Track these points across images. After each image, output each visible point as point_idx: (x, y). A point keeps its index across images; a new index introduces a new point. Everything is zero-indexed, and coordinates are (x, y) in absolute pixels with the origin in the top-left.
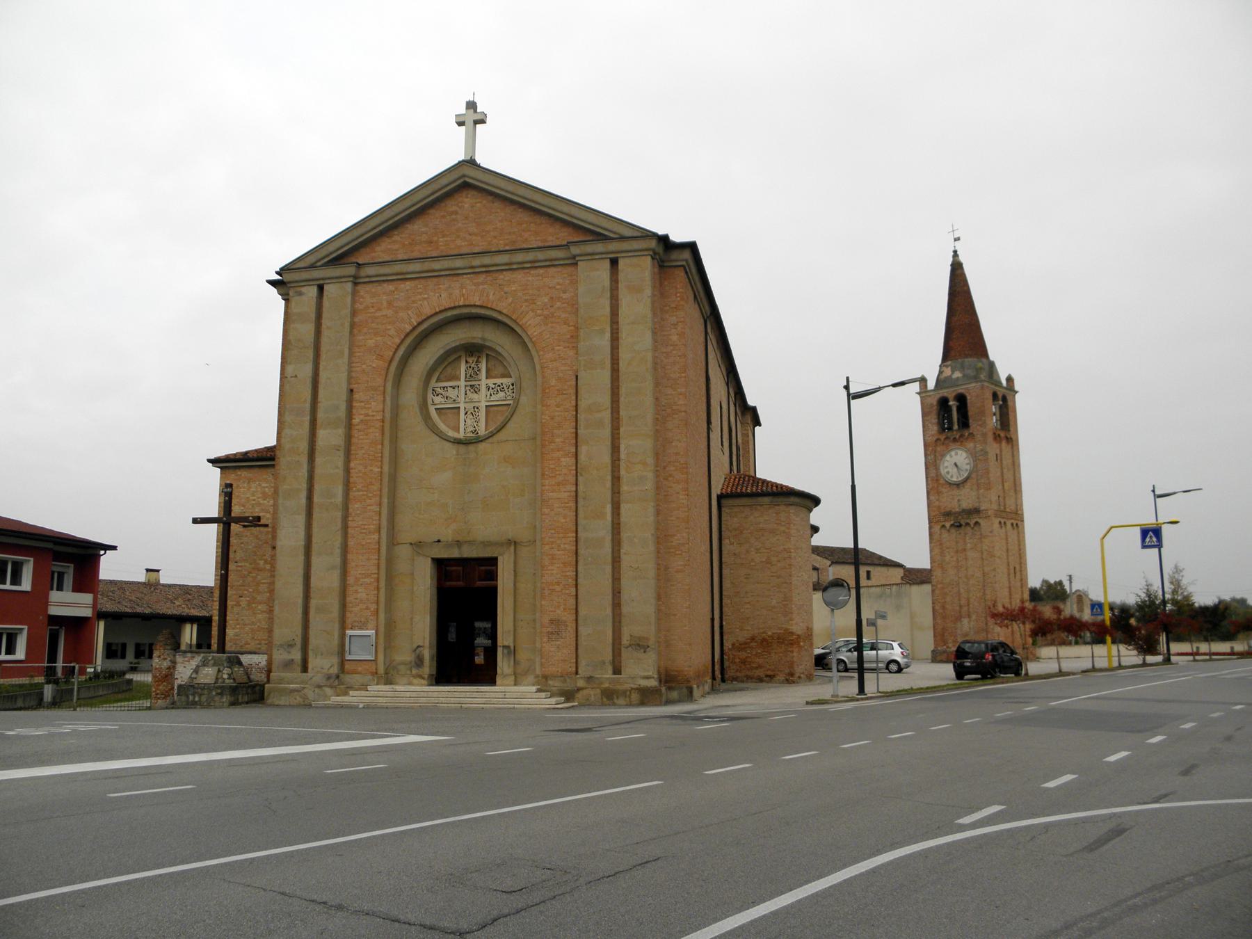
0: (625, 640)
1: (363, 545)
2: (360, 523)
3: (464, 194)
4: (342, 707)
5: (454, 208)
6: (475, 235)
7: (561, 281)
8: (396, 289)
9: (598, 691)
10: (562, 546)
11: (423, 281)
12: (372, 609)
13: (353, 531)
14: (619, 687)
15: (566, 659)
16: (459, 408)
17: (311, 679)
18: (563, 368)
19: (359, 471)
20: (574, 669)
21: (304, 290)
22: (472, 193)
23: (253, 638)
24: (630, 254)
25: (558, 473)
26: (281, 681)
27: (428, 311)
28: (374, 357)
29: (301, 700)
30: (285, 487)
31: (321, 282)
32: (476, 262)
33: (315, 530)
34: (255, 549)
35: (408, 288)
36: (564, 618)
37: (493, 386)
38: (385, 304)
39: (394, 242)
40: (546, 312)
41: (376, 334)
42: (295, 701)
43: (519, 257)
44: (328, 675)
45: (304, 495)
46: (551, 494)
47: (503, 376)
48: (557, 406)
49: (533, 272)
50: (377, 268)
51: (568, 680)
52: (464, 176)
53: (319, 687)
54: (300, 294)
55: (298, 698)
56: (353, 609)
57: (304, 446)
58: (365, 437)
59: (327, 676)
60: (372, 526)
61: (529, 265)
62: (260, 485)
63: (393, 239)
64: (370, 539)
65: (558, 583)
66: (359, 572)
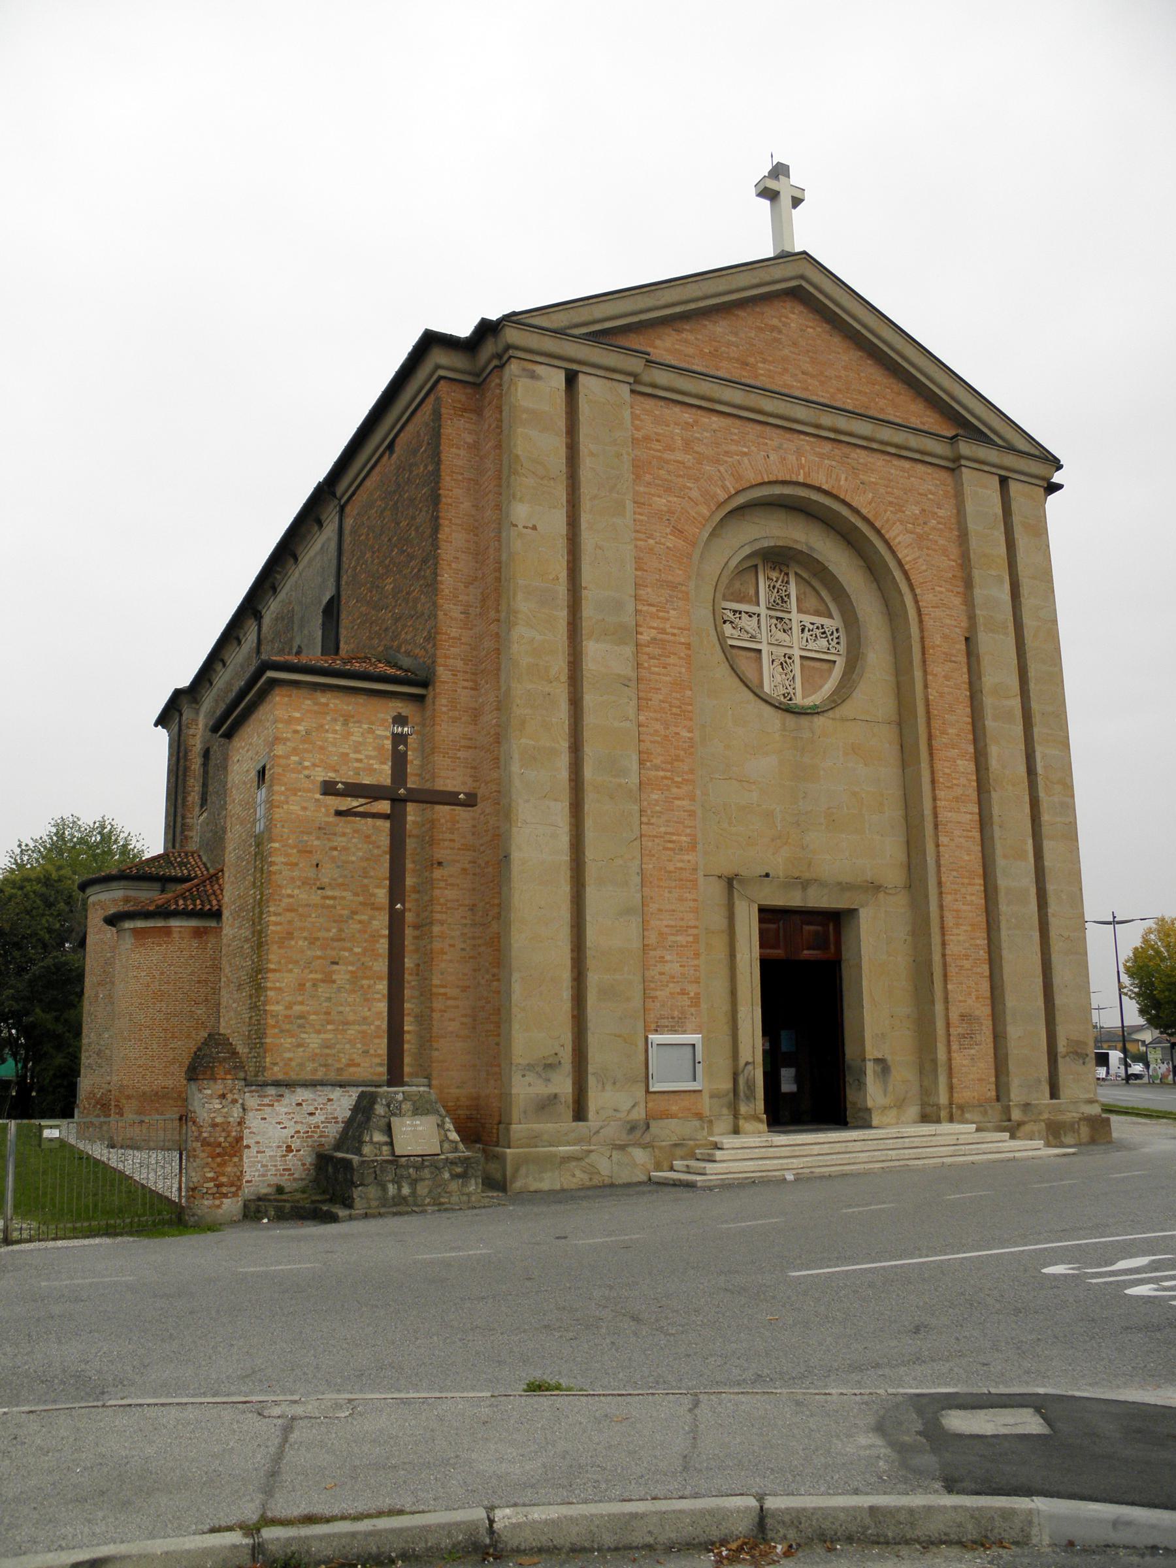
0: (1062, 1048)
1: (670, 872)
2: (663, 829)
3: (789, 305)
4: (754, 1182)
5: (775, 322)
6: (812, 376)
7: (933, 488)
8: (696, 422)
9: (1043, 1124)
10: (968, 898)
11: (738, 422)
12: (692, 994)
13: (650, 844)
14: (1060, 1118)
15: (984, 1077)
16: (759, 651)
17: (598, 1132)
18: (948, 621)
19: (656, 731)
20: (994, 1093)
21: (540, 370)
22: (799, 308)
23: (366, 1052)
24: (1023, 478)
25: (955, 782)
26: (534, 1139)
27: (752, 477)
28: (668, 530)
29: (586, 1177)
30: (523, 741)
31: (575, 367)
32: (827, 419)
33: (590, 835)
34: (365, 864)
35: (714, 426)
36: (977, 1013)
37: (811, 627)
38: (679, 442)
39: (686, 341)
40: (918, 530)
41: (668, 490)
42: (575, 1180)
43: (886, 434)
44: (628, 1122)
45: (563, 762)
46: (950, 814)
47: (817, 613)
48: (947, 677)
49: (896, 462)
50: (672, 376)
51: (990, 1112)
52: (802, 277)
53: (622, 1148)
54: (533, 376)
55: (578, 1173)
56: (658, 993)
57: (559, 665)
58: (663, 671)
59: (628, 1127)
60: (684, 838)
61: (893, 450)
62: (371, 731)
63: (684, 335)
64: (682, 861)
65: (967, 957)
66: (665, 923)
